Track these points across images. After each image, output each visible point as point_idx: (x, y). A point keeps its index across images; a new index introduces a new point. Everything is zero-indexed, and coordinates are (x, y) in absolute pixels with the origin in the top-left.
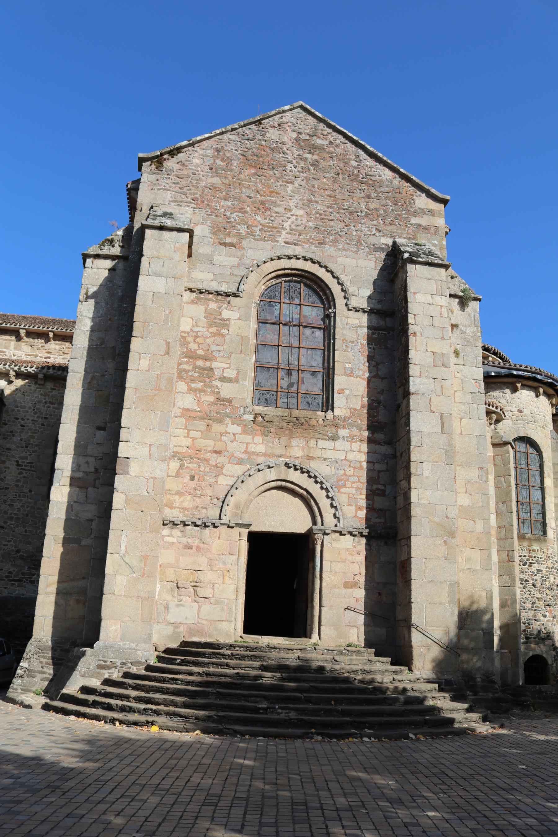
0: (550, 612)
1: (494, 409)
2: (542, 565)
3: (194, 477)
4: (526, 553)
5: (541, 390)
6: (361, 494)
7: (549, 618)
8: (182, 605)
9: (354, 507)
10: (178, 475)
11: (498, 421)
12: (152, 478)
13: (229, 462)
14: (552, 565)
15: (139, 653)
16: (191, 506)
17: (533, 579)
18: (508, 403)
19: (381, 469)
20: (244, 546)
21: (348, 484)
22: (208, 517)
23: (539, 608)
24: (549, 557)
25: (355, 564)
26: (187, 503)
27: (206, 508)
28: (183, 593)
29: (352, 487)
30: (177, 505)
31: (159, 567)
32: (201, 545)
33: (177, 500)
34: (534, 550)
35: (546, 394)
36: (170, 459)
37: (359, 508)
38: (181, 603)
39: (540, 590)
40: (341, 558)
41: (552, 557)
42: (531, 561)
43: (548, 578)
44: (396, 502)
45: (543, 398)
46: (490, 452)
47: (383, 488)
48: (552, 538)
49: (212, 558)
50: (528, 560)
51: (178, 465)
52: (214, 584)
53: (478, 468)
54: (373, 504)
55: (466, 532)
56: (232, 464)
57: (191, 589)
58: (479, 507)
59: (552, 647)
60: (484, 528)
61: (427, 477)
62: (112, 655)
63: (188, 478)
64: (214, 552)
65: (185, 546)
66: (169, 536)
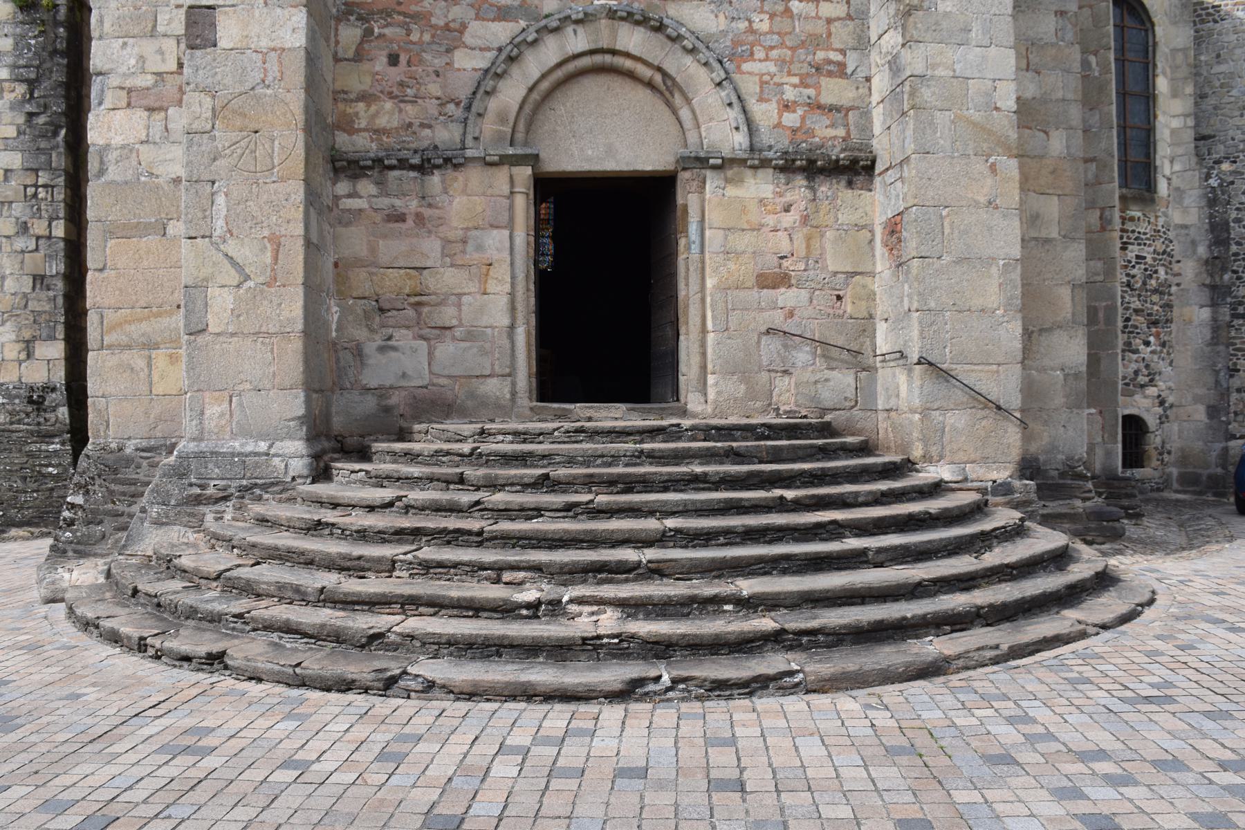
0: (1157, 335)
2: (1146, 248)
3: (398, 56)
6: (789, 74)
7: (1154, 348)
8: (394, 349)
9: (774, 105)
10: (359, 57)
12: (274, 49)
13: (478, 18)
15: (276, 461)
16: (395, 124)
17: (1128, 275)
19: (834, 15)
20: (522, 206)
21: (759, 54)
22: (436, 147)
23: (1137, 327)
24: (1159, 231)
25: (779, 233)
26: (387, 117)
27: (430, 127)
28: (391, 322)
29: (767, 59)
30: (363, 124)
31: (330, 265)
32: (427, 212)
33: (362, 114)
34: (1132, 219)
36: (338, 20)
37: (787, 106)
38: (390, 343)
39: (1139, 296)
40: (748, 222)
41: (1164, 233)
43: (1156, 272)
44: (870, 89)
47: (839, 58)
49: (453, 239)
51: (358, 32)
52: (460, 295)
53: (1056, 13)
54: (819, 94)
55: (1028, 156)
56: (484, 20)
57: (410, 312)
58: (1057, 100)
59: (1157, 401)
60: (1068, 147)
61: (946, 14)
62: (216, 470)
63: (385, 60)
64: (455, 224)
65: (387, 215)
66: (350, 196)
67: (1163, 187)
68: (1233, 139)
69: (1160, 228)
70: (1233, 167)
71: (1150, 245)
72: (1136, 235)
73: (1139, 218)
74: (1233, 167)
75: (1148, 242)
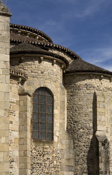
1: (20, 75)
2: (50, 156)
4: (41, 149)
5: (55, 61)
11: (22, 82)
14: (56, 155)
18: (36, 68)
34: (46, 148)
35: (57, 63)
39: (48, 169)
41: (56, 151)
42: (44, 154)
43: (53, 162)
45: (55, 65)
46: (16, 98)
48: (57, 141)
50: (42, 153)
53: (4, 109)
60: (5, 141)
67: (56, 139)
68: (83, 123)
69: (55, 150)
71: (51, 155)
72: (47, 152)
73: (48, 148)
74: (83, 131)
75: (50, 154)
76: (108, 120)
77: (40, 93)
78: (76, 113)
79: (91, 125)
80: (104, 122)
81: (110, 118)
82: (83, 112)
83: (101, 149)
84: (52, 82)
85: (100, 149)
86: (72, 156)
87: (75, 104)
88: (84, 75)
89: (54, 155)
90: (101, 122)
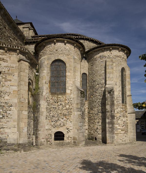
1: (17, 48)
5: (66, 41)
34: (59, 98)
50: (56, 101)
67: (68, 91)
70: (98, 86)
74: (98, 86)
76: (117, 77)
77: (57, 63)
78: (94, 76)
79: (104, 81)
80: (112, 78)
81: (119, 75)
82: (98, 74)
83: (108, 96)
84: (65, 55)
85: (107, 96)
86: (79, 101)
87: (94, 70)
88: (99, 50)
89: (67, 102)
90: (110, 78)
